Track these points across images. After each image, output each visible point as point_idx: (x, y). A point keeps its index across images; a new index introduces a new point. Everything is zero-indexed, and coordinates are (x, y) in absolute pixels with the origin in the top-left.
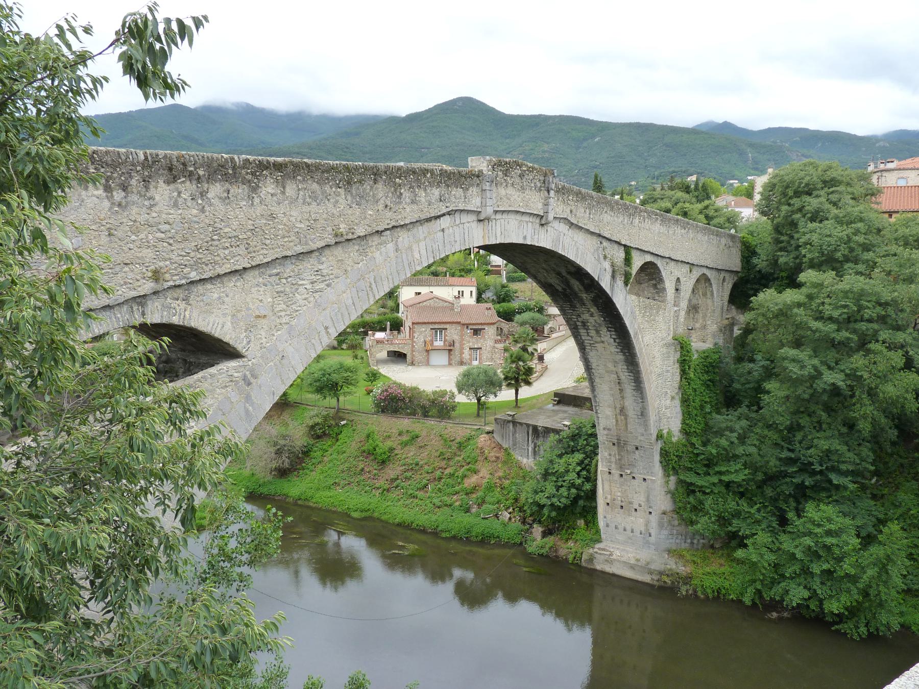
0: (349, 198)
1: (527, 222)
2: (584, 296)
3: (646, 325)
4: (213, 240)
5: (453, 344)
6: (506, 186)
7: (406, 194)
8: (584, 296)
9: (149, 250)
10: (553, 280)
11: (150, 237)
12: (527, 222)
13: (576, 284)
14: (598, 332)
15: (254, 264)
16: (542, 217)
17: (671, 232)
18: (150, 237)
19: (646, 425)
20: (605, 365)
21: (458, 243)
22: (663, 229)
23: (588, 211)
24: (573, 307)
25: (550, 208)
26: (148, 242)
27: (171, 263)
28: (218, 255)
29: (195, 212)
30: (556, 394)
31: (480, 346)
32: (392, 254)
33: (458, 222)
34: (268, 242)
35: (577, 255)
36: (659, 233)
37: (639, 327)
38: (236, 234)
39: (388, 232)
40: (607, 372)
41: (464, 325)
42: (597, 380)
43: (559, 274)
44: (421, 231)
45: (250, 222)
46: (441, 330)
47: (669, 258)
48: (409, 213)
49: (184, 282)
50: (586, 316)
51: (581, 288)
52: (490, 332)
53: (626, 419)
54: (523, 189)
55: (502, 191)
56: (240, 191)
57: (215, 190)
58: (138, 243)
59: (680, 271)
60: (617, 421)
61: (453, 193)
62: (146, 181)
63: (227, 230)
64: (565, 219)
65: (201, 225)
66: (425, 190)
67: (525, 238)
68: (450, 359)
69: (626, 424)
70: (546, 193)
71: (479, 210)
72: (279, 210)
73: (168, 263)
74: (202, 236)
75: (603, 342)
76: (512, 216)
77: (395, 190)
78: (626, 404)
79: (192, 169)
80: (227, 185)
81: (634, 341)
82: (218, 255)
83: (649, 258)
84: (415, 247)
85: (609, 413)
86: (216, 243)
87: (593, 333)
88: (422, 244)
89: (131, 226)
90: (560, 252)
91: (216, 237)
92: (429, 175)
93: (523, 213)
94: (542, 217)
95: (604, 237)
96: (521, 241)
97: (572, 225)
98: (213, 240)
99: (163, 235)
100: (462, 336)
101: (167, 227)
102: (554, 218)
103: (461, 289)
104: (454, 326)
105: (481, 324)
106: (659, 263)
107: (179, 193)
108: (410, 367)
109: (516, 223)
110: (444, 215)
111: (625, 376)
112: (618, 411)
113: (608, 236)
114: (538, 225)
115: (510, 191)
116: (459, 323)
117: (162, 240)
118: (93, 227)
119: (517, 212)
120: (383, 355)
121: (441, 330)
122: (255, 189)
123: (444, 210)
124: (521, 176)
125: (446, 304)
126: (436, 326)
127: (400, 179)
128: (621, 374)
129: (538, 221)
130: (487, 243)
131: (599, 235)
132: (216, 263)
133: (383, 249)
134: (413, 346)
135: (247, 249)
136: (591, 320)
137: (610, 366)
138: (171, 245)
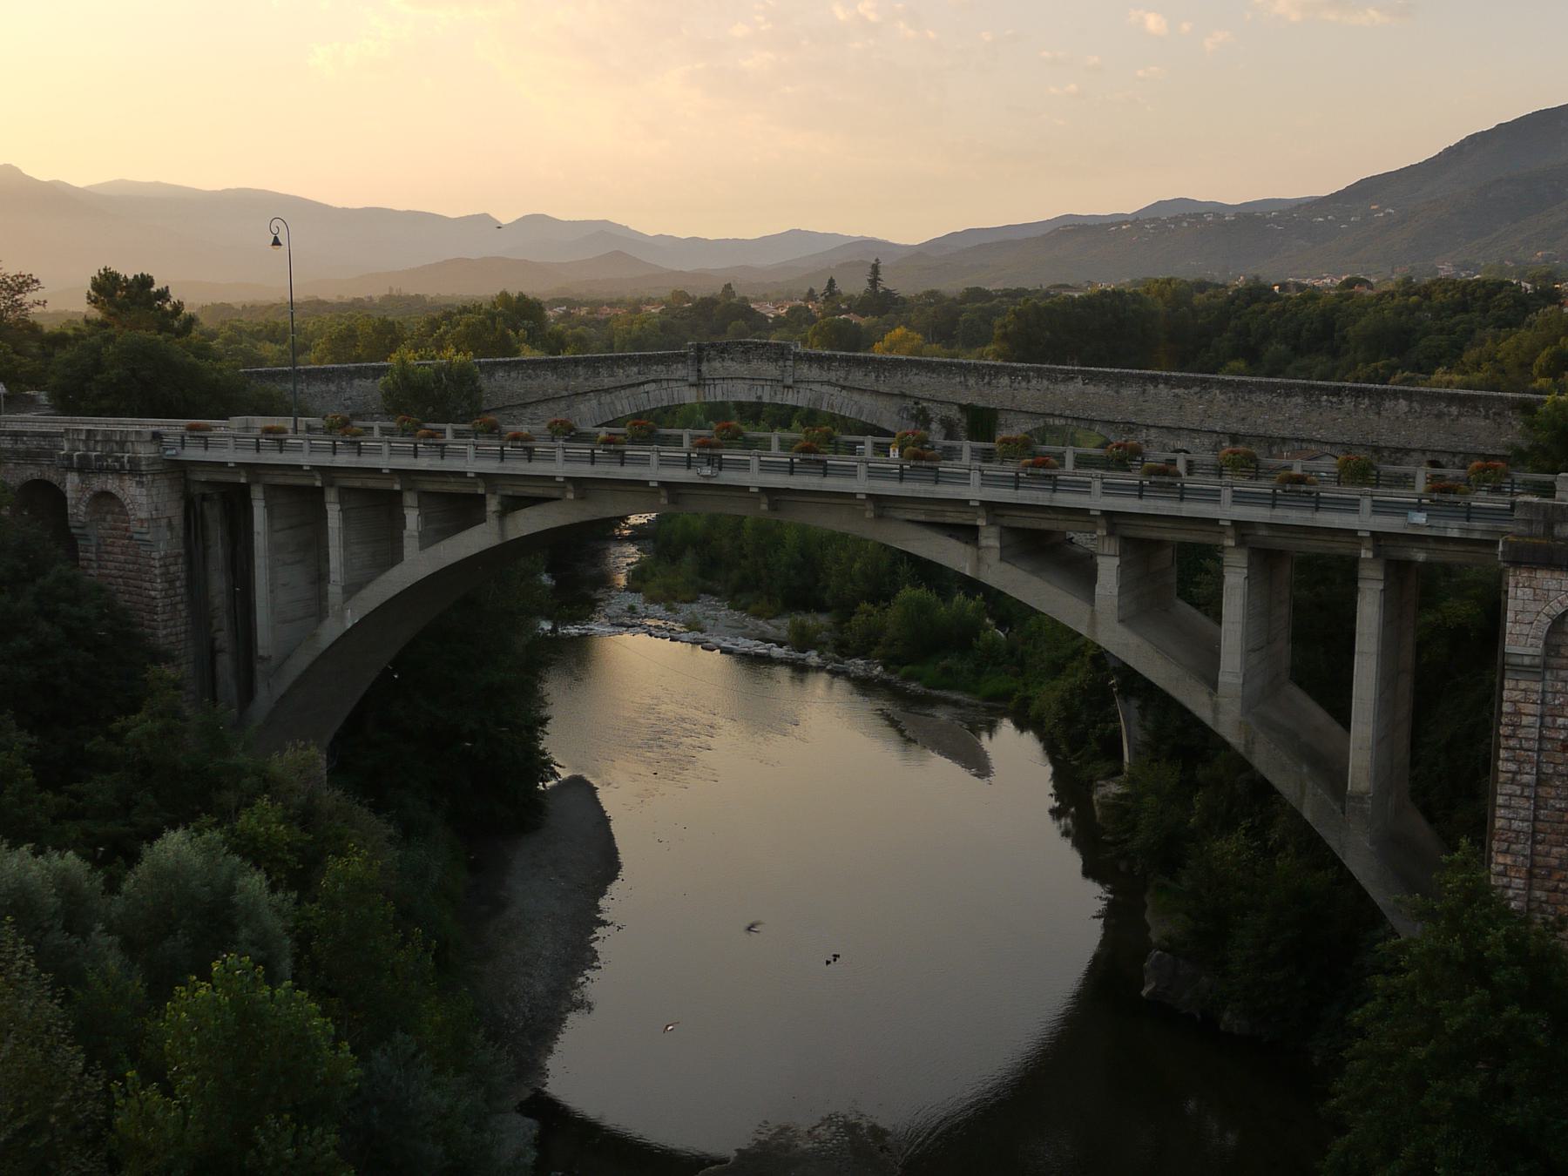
0: (555, 377)
6: (723, 360)
7: (603, 372)
12: (763, 386)
23: (873, 375)
39: (592, 394)
48: (607, 382)
54: (749, 361)
55: (717, 364)
66: (623, 368)
67: (760, 397)
77: (594, 370)
84: (616, 402)
95: (919, 398)
109: (747, 387)
115: (728, 363)
119: (745, 379)
133: (587, 404)
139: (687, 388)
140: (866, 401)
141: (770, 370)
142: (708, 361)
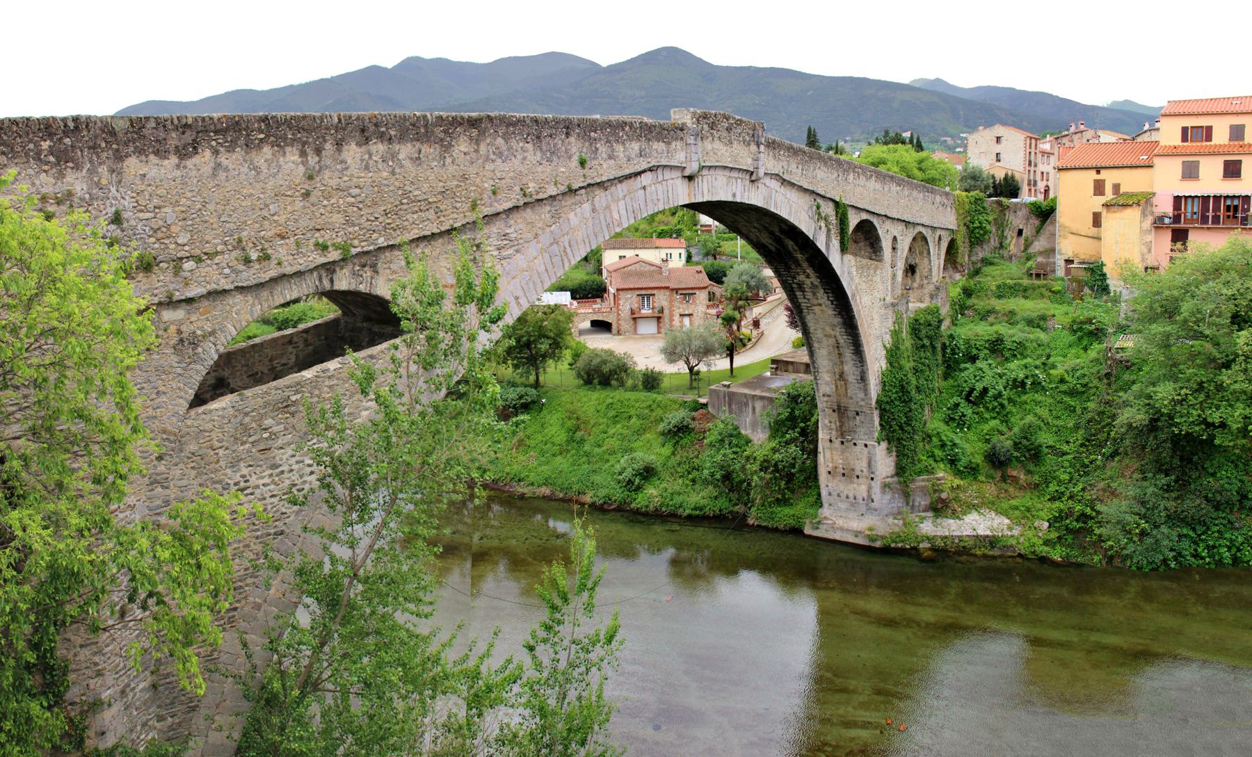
1: (736, 178)
2: (799, 256)
3: (864, 286)
4: (403, 204)
5: (662, 311)
7: (603, 149)
8: (799, 256)
9: (340, 216)
10: (766, 239)
11: (341, 201)
12: (736, 178)
13: (790, 244)
14: (814, 294)
15: (443, 229)
16: (752, 173)
17: (886, 189)
18: (341, 201)
19: (866, 390)
20: (823, 329)
21: (661, 202)
22: (878, 186)
23: (800, 167)
24: (788, 268)
25: (761, 163)
26: (339, 207)
27: (360, 229)
28: (407, 220)
29: (385, 174)
30: (774, 361)
31: (690, 312)
32: (587, 215)
33: (660, 178)
34: (458, 205)
35: (790, 213)
36: (875, 190)
37: (856, 288)
38: (425, 197)
40: (826, 336)
41: (673, 290)
42: (816, 345)
43: (772, 233)
44: (621, 189)
45: (441, 184)
46: (649, 296)
47: (886, 216)
48: (606, 170)
49: (371, 248)
50: (802, 277)
51: (796, 248)
52: (702, 296)
53: (846, 384)
55: (708, 145)
56: (432, 150)
57: (405, 151)
58: (329, 208)
59: (897, 229)
60: (837, 386)
61: (655, 147)
62: (339, 144)
63: (416, 193)
64: (777, 175)
65: (391, 188)
67: (734, 195)
68: (659, 328)
69: (846, 389)
70: (755, 147)
71: (684, 165)
72: (472, 170)
73: (357, 228)
74: (392, 200)
75: (820, 305)
76: (720, 172)
77: (591, 144)
78: (846, 368)
79: (383, 129)
80: (418, 145)
81: (852, 303)
82: (407, 220)
83: (864, 216)
84: (614, 207)
85: (828, 379)
86: (405, 207)
87: (809, 295)
88: (622, 203)
89: (323, 191)
90: (772, 210)
91: (405, 201)
92: (627, 128)
93: (732, 169)
94: (752, 173)
95: (818, 194)
96: (730, 199)
97: (784, 182)
98: (403, 204)
99: (353, 200)
100: (671, 302)
101: (357, 191)
102: (765, 174)
103: (669, 251)
104: (662, 291)
105: (692, 289)
106: (875, 221)
107: (370, 155)
108: (616, 337)
110: (644, 171)
111: (843, 339)
112: (837, 376)
113: (823, 193)
114: (748, 182)
116: (667, 288)
117: (352, 205)
118: (289, 193)
119: (725, 168)
120: (587, 325)
121: (649, 296)
122: (447, 148)
123: (644, 166)
124: (729, 130)
125: (653, 268)
126: (643, 292)
127: (595, 132)
128: (839, 338)
129: (748, 177)
130: (693, 201)
131: (813, 192)
132: (404, 228)
134: (619, 314)
135: (436, 213)
136: (808, 282)
137: (828, 329)
138: (360, 209)
139: (680, 180)
140: (793, 195)
141: (743, 156)
142: (702, 138)
